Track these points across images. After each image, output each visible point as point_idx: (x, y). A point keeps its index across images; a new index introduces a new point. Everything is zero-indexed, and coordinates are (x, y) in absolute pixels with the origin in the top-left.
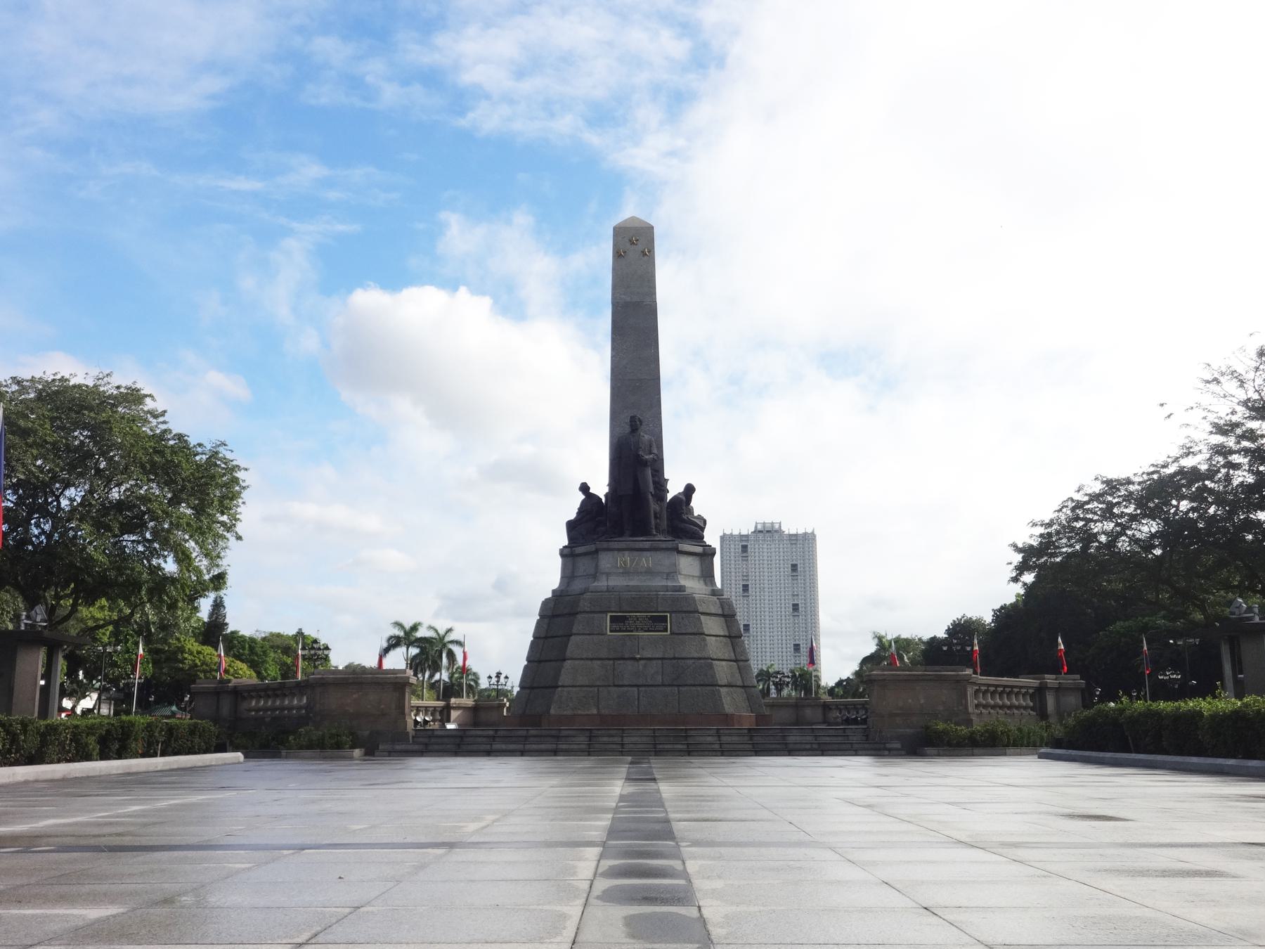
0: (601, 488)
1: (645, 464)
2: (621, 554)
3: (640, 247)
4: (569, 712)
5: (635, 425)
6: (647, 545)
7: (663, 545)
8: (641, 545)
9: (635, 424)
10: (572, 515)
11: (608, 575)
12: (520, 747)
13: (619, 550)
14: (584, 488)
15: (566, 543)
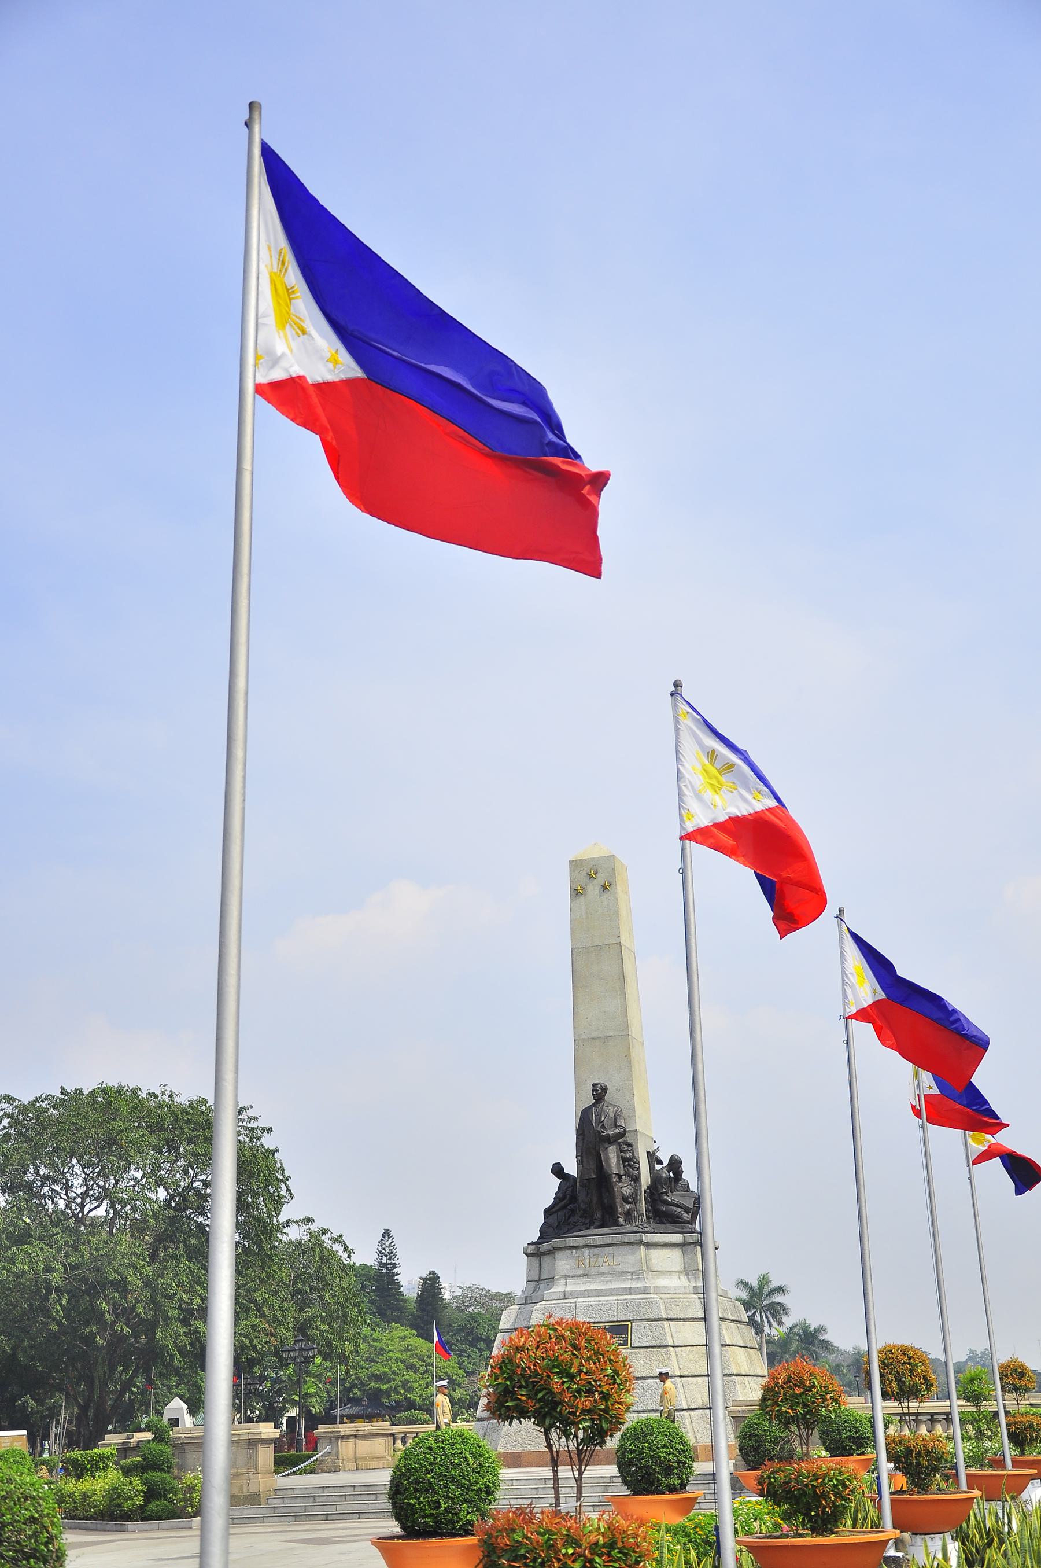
0: (571, 1168)
1: (609, 1140)
2: (579, 1252)
3: (601, 879)
4: (518, 1449)
5: (599, 1093)
6: (607, 1239)
7: (626, 1238)
8: (599, 1240)
9: (599, 1093)
10: (549, 1201)
11: (566, 1277)
12: (363, 1508)
13: (576, 1248)
14: (558, 1170)
15: (535, 1236)
